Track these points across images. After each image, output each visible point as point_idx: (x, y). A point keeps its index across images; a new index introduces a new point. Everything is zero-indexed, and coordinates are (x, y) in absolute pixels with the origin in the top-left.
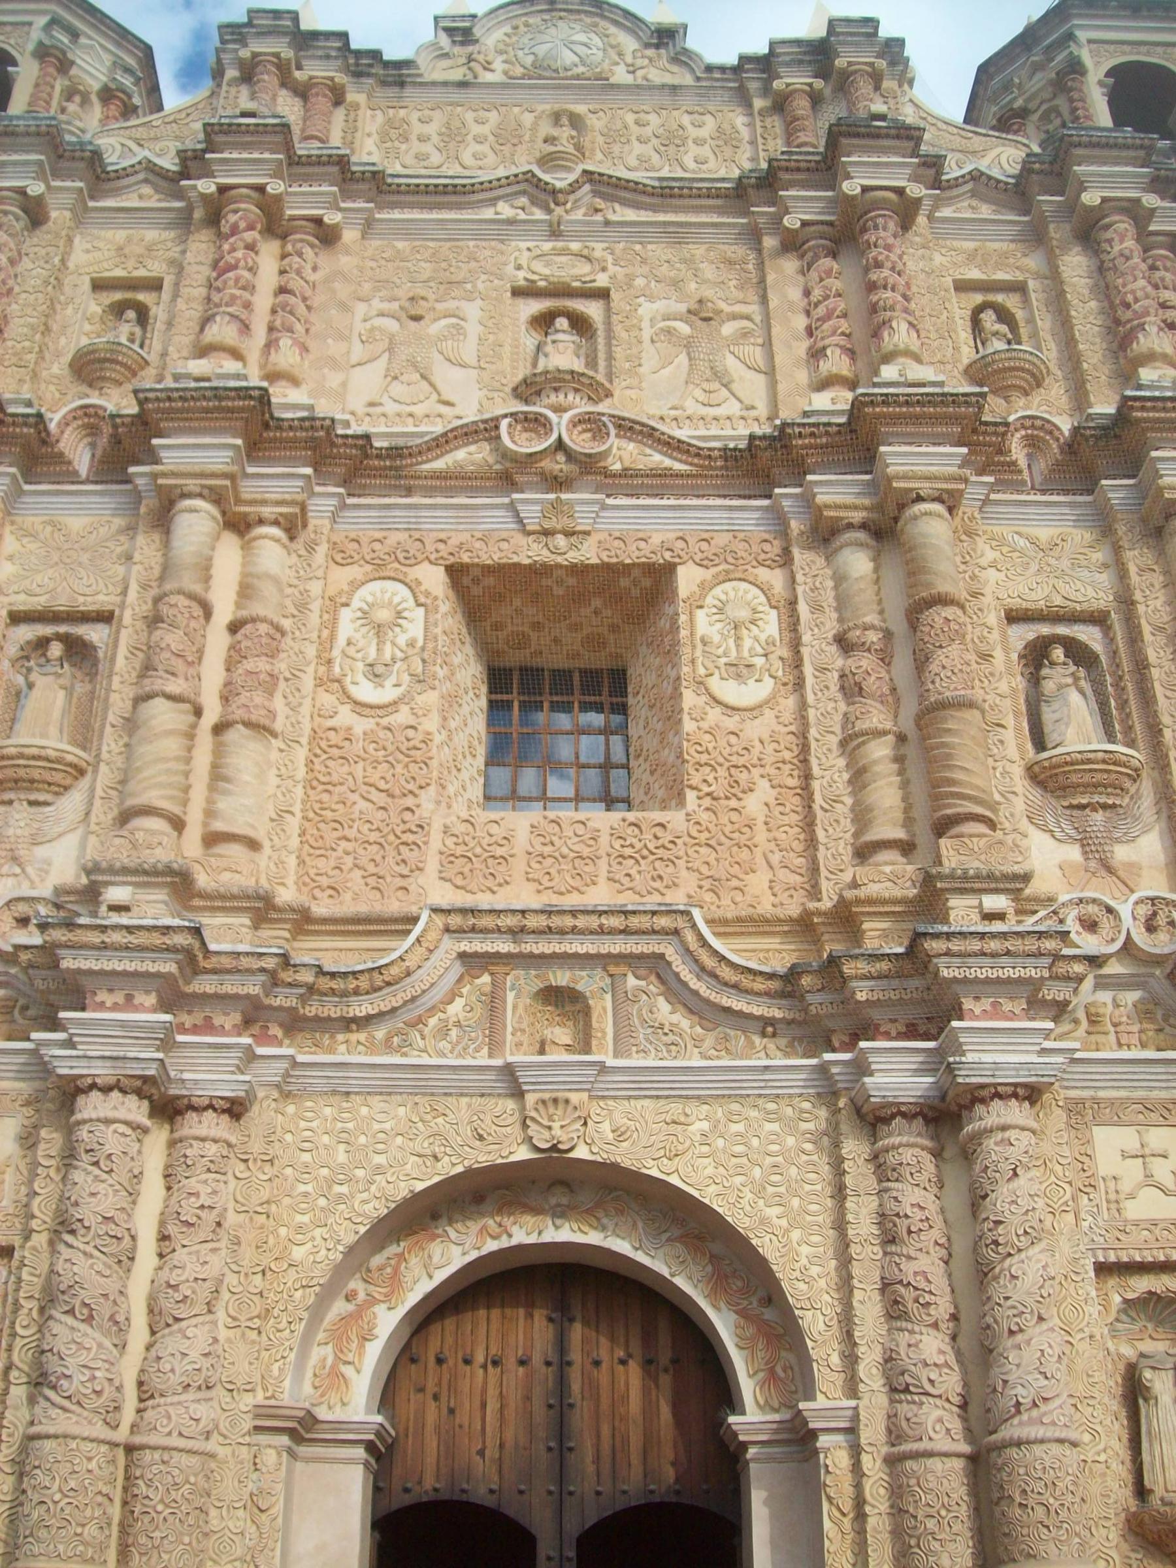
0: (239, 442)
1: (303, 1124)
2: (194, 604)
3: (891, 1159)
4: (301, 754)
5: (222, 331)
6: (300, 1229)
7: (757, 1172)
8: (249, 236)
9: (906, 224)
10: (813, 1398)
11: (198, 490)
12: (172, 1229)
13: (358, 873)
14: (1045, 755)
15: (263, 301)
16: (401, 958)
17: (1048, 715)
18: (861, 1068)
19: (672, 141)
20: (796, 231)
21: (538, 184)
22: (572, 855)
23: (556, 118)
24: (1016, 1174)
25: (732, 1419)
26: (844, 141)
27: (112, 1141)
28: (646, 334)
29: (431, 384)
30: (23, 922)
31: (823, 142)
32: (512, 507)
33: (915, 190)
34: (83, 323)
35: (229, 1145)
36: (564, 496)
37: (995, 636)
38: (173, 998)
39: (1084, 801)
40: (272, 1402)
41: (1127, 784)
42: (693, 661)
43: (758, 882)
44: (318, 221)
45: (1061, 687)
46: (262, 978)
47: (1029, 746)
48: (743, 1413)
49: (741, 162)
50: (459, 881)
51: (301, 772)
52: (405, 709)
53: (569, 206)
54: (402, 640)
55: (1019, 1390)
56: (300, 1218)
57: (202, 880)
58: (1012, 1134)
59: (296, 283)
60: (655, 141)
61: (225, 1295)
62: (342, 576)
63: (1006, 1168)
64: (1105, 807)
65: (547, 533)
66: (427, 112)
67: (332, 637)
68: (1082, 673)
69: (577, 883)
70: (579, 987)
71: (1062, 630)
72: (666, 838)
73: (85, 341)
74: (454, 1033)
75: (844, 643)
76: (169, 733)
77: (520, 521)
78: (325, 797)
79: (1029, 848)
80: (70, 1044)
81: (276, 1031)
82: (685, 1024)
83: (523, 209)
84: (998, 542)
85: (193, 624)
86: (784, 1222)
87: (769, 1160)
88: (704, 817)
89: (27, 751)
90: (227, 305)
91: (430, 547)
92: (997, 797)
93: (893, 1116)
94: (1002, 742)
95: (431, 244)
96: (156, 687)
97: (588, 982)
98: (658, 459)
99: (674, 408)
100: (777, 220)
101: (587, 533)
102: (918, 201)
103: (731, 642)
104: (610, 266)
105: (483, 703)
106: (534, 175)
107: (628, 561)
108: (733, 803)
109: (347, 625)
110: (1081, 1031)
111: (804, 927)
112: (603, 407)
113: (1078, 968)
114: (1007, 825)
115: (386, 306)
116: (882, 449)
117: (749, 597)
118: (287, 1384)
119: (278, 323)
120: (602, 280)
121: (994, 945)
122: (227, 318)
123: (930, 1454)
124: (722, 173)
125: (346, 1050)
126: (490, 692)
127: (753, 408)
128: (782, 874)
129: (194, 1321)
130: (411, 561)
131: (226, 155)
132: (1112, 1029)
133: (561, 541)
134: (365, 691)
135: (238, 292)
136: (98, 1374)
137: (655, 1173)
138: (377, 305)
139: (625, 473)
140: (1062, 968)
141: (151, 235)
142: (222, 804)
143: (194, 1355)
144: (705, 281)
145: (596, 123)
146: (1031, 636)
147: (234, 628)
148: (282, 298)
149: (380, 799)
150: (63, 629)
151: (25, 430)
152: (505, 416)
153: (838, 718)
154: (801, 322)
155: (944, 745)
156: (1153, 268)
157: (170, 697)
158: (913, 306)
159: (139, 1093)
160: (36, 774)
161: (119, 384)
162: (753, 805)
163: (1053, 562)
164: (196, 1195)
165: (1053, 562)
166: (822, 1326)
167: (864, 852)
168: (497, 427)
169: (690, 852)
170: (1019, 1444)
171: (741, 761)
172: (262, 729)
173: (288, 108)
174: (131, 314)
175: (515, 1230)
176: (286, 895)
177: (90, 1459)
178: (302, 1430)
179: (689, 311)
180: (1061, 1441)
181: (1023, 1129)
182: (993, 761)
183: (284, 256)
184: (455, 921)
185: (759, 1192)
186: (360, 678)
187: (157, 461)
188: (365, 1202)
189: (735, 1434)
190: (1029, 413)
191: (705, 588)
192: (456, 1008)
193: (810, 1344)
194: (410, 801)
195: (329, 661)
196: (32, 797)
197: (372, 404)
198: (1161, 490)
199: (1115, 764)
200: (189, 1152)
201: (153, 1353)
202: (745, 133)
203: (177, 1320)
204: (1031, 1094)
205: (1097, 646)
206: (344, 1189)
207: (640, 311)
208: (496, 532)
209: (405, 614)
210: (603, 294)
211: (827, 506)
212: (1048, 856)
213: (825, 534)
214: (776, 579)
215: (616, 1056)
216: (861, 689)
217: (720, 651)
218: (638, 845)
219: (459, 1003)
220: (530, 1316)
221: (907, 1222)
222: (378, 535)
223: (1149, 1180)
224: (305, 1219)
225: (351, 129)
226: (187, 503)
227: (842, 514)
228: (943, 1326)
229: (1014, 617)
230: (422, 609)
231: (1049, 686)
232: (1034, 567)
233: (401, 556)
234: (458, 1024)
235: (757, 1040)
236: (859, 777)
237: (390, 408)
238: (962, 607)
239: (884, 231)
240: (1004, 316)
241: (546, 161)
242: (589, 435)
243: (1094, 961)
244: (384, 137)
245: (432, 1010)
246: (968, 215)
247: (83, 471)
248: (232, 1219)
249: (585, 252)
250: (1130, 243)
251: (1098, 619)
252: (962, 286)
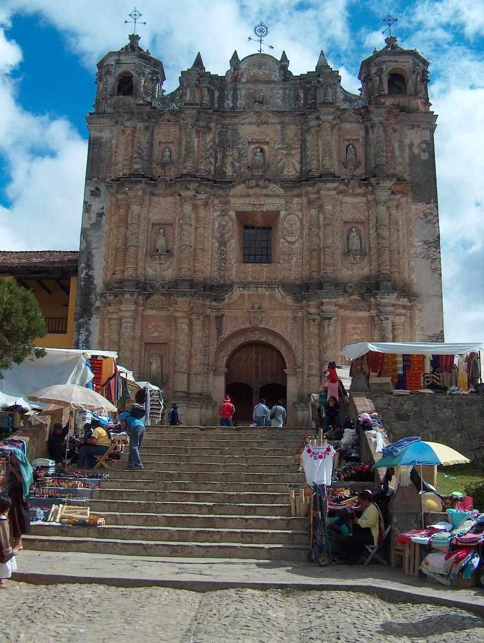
30: (163, 287)
120: (267, 140)
150: (162, 226)
202: (302, 95)
214: (300, 214)
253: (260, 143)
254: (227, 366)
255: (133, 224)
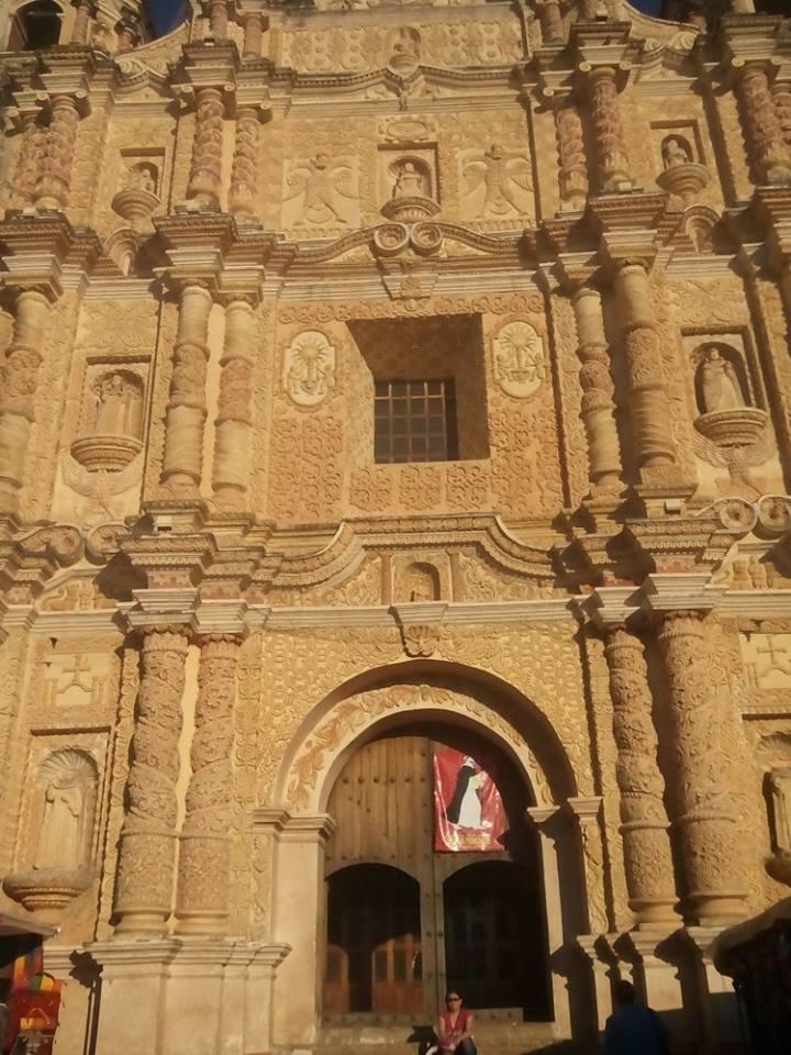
0: (218, 250)
1: (277, 647)
2: (199, 350)
3: (617, 655)
4: (267, 436)
5: (201, 181)
6: (278, 707)
7: (538, 664)
8: (216, 119)
9: (620, 88)
10: (576, 795)
11: (196, 281)
12: (203, 711)
13: (303, 503)
14: (706, 415)
15: (227, 160)
16: (329, 550)
17: (708, 391)
18: (595, 603)
19: (472, 44)
20: (550, 97)
21: (389, 75)
22: (425, 487)
23: (402, 31)
24: (691, 662)
25: (529, 809)
26: (581, 35)
27: (167, 662)
28: (461, 170)
29: (332, 210)
30: (109, 539)
31: (567, 37)
32: (383, 283)
33: (625, 65)
34: (117, 176)
35: (235, 661)
36: (413, 276)
37: (674, 345)
38: (197, 576)
39: (730, 442)
40: (264, 808)
41: (758, 430)
42: (492, 371)
43: (534, 497)
44: (257, 108)
45: (716, 374)
46: (251, 564)
47: (697, 413)
48: (536, 805)
49: (516, 57)
50: (360, 504)
51: (267, 447)
52: (326, 407)
53: (410, 90)
54: (322, 367)
55: (698, 789)
56: (277, 701)
57: (212, 509)
58: (689, 639)
59: (247, 149)
60: (462, 44)
61: (236, 747)
62: (284, 330)
63: (685, 659)
64: (743, 445)
65: (404, 298)
66: (321, 33)
67: (282, 367)
68: (729, 365)
69: (429, 503)
70: (432, 563)
71: (717, 339)
72: (479, 475)
73: (119, 189)
74: (361, 592)
75: (583, 356)
76: (189, 426)
77: (388, 292)
78: (282, 460)
79: (696, 472)
80: (138, 608)
81: (259, 594)
82: (493, 581)
83: (382, 94)
84: (677, 287)
85: (199, 362)
86: (555, 693)
87: (545, 658)
88: (502, 461)
89: (104, 440)
90: (206, 164)
91: (337, 310)
92: (677, 442)
93: (617, 630)
94: (678, 409)
95: (327, 119)
96: (179, 400)
97: (436, 558)
98: (469, 250)
99: (478, 217)
100: (538, 93)
101: (428, 297)
102: (628, 71)
103: (515, 359)
104: (436, 127)
105: (372, 401)
106: (389, 71)
107: (453, 313)
108: (518, 453)
109: (290, 359)
110: (730, 579)
111: (560, 524)
112: (436, 218)
113: (727, 541)
114: (681, 458)
115: (302, 161)
116: (604, 234)
117: (525, 330)
118: (272, 796)
119: (237, 175)
120: (432, 138)
121: (674, 529)
122: (205, 173)
123: (647, 827)
124: (505, 61)
125: (299, 603)
126: (377, 395)
127: (526, 214)
128: (548, 493)
129: (218, 763)
130: (326, 319)
131: (197, 67)
132: (749, 576)
133: (413, 303)
134: (302, 398)
135: (209, 155)
136: (162, 796)
137: (479, 667)
138: (297, 160)
139: (450, 259)
140: (715, 540)
141: (155, 121)
142: (223, 467)
143: (218, 782)
144: (497, 134)
145: (425, 34)
146: (698, 344)
147: (223, 363)
148: (238, 158)
149: (315, 460)
150: (122, 367)
151: (88, 247)
152: (377, 228)
153: (579, 400)
154: (555, 156)
155: (641, 413)
156: (779, 105)
157: (190, 406)
158: (624, 141)
159: (181, 632)
160: (110, 453)
161: (144, 216)
162: (530, 453)
163: (712, 298)
164: (217, 690)
165: (712, 298)
166: (579, 753)
167: (596, 477)
168: (372, 235)
169: (494, 482)
170: (699, 820)
171: (522, 429)
172: (244, 422)
173: (234, 32)
174: (147, 172)
175: (400, 702)
176: (261, 517)
177: (159, 846)
178: (280, 821)
179: (487, 154)
180: (723, 818)
181: (695, 636)
182: (670, 420)
183: (238, 131)
184: (359, 527)
185: (539, 676)
186: (299, 390)
187: (171, 264)
188: (314, 689)
189: (532, 819)
190: (698, 205)
191: (498, 327)
192: (363, 576)
193: (572, 763)
194: (331, 460)
195: (280, 381)
196: (110, 467)
197: (296, 224)
198: (780, 248)
199: (751, 419)
200: (211, 666)
201: (194, 784)
203: (208, 763)
204: (702, 614)
205: (740, 348)
206: (302, 683)
207: (456, 156)
208: (373, 298)
209: (324, 351)
210: (434, 146)
211: (571, 273)
212: (708, 475)
213: (569, 290)
215: (454, 601)
216: (592, 382)
217: (508, 364)
218: (463, 480)
219: (364, 574)
220: (411, 752)
221: (626, 691)
222: (306, 304)
223: (775, 665)
224: (281, 701)
225: (274, 46)
226: (190, 288)
227: (579, 276)
228: (651, 752)
229: (687, 332)
230: (333, 348)
231: (708, 374)
232: (699, 302)
233: (319, 317)
234: (364, 586)
235: (536, 588)
236: (591, 436)
237: (309, 225)
238: (653, 329)
239: (607, 92)
240: (683, 143)
241: (394, 62)
242: (427, 237)
243: (737, 537)
244: (295, 50)
245: (349, 579)
246: (660, 79)
247: (126, 272)
248: (237, 703)
249: (422, 120)
250: (763, 89)
251: (741, 331)
252: (656, 126)
253: (410, 146)
254: (331, 802)
255: (20, 348)
